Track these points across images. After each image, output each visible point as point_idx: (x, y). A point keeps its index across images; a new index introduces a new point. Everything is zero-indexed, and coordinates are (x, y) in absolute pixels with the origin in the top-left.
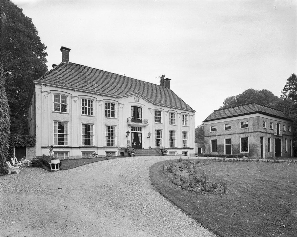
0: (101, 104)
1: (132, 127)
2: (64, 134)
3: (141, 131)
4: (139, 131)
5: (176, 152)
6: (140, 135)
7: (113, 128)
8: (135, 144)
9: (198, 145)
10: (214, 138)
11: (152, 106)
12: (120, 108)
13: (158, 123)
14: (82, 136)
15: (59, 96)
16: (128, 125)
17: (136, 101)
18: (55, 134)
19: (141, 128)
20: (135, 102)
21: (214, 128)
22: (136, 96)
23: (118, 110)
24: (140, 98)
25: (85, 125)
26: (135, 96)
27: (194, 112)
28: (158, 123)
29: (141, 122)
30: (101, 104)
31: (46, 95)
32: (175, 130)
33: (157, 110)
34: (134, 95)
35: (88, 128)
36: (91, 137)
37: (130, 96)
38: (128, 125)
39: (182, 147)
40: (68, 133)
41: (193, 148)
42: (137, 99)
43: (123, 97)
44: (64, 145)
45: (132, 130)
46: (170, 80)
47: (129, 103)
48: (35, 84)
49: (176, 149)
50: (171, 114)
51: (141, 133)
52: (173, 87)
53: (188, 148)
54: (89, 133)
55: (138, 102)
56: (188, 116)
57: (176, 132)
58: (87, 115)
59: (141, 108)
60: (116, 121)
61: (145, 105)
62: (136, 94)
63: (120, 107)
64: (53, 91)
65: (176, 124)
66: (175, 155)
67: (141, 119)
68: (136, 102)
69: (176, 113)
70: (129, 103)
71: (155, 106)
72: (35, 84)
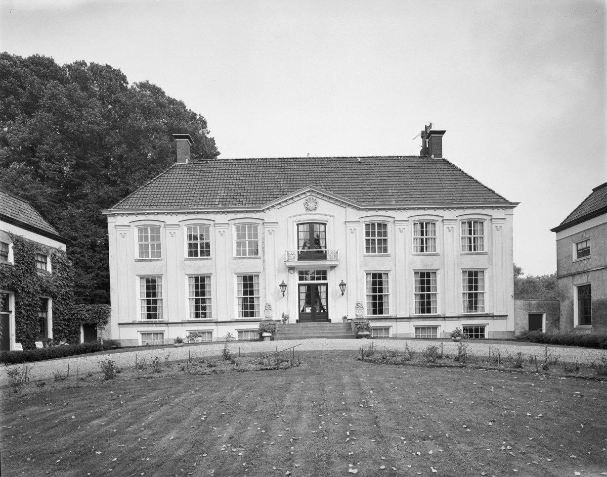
0: (224, 230)
1: (301, 273)
2: (383, 294)
3: (325, 278)
4: (318, 279)
5: (439, 327)
6: (323, 288)
7: (431, 274)
8: (308, 310)
9: (529, 305)
10: (582, 280)
11: (353, 214)
12: (267, 233)
13: (377, 253)
14: (414, 295)
15: (146, 229)
16: (289, 268)
17: (307, 209)
18: (415, 294)
19: (325, 272)
20: (304, 211)
21: (584, 245)
22: (307, 198)
23: (263, 239)
24: (318, 200)
25: (243, 276)
26: (305, 199)
27: (511, 206)
28: (377, 253)
29: (322, 256)
30: (224, 230)
31: (123, 232)
32: (434, 267)
33: (373, 222)
34: (303, 196)
35: (200, 284)
36: (158, 302)
37: (291, 201)
38: (289, 268)
39: (462, 312)
40: (486, 290)
41: (506, 316)
42: (311, 205)
43: (273, 206)
44: (255, 318)
45: (301, 279)
46: (443, 132)
47: (290, 217)
48: (106, 216)
49: (439, 319)
50: (423, 227)
51: (326, 285)
52: (450, 151)
53: (486, 316)
54: (381, 290)
55: (314, 212)
56: (485, 224)
57: (438, 272)
58: (199, 257)
59: (325, 224)
60: (260, 261)
61: (333, 216)
62: (309, 194)
63: (266, 230)
64: (134, 223)
65: (486, 250)
66: (388, 338)
67: (326, 251)
68: (309, 212)
69: (486, 219)
70: (290, 217)
71: (364, 213)
72: (106, 216)
